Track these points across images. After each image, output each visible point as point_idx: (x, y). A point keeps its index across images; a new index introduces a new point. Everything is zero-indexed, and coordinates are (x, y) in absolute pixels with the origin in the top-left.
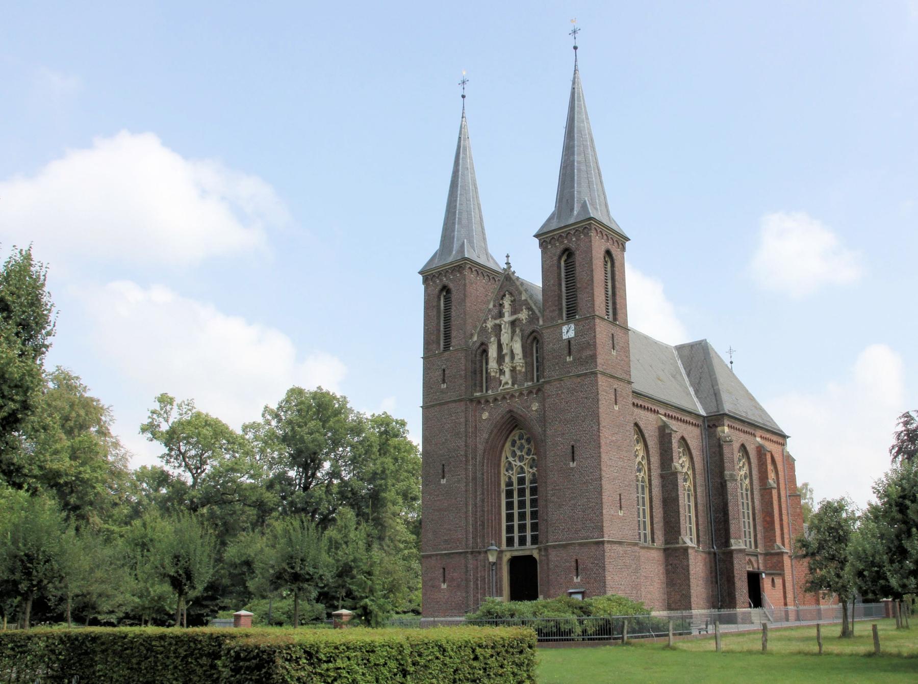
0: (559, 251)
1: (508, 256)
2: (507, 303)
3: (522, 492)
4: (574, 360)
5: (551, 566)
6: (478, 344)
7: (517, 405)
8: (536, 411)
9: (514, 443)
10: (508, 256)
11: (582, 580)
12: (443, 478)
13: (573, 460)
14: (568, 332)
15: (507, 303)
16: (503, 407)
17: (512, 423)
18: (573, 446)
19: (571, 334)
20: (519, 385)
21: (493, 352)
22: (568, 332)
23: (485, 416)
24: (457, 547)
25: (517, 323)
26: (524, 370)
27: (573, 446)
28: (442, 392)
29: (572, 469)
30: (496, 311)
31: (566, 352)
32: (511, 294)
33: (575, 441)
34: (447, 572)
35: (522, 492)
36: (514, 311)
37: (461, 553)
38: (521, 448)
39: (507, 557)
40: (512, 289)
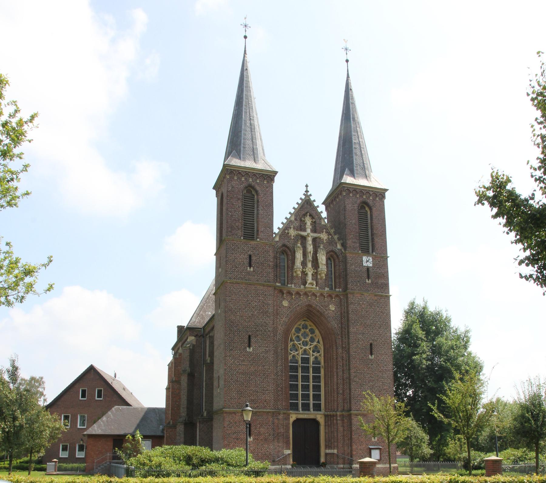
0: (358, 202)
1: (307, 186)
2: (308, 221)
3: (305, 369)
4: (372, 283)
5: (353, 428)
6: (280, 244)
7: (316, 302)
8: (333, 311)
9: (298, 330)
10: (307, 186)
11: (378, 440)
12: (249, 346)
13: (371, 354)
14: (367, 261)
15: (308, 221)
16: (303, 300)
17: (311, 315)
18: (371, 344)
19: (370, 265)
20: (320, 288)
21: (299, 256)
22: (367, 261)
23: (285, 303)
24: (265, 407)
25: (318, 240)
26: (324, 278)
27: (371, 344)
28: (249, 273)
29: (371, 360)
30: (297, 224)
31: (365, 275)
32: (310, 215)
33: (373, 340)
34: (253, 428)
35: (305, 369)
36: (314, 230)
37: (270, 412)
38: (305, 335)
39: (293, 417)
40: (314, 215)
